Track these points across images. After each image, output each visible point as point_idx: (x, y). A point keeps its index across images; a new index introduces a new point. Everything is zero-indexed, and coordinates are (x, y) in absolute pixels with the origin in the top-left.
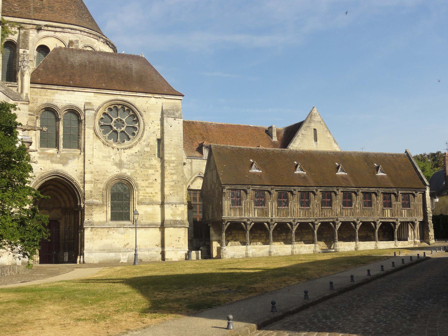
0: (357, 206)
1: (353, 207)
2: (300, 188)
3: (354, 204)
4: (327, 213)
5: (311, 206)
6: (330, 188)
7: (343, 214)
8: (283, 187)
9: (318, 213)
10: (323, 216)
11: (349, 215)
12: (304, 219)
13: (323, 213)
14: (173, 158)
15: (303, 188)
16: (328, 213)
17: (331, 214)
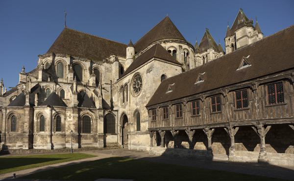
0: (256, 104)
1: (249, 107)
2: (188, 98)
3: (250, 103)
4: (216, 118)
5: (200, 114)
6: (215, 90)
7: (235, 118)
8: (176, 101)
9: (207, 120)
10: (213, 122)
11: (244, 118)
12: (195, 126)
13: (213, 119)
14: (149, 95)
15: (190, 97)
16: (217, 118)
17: (220, 118)
